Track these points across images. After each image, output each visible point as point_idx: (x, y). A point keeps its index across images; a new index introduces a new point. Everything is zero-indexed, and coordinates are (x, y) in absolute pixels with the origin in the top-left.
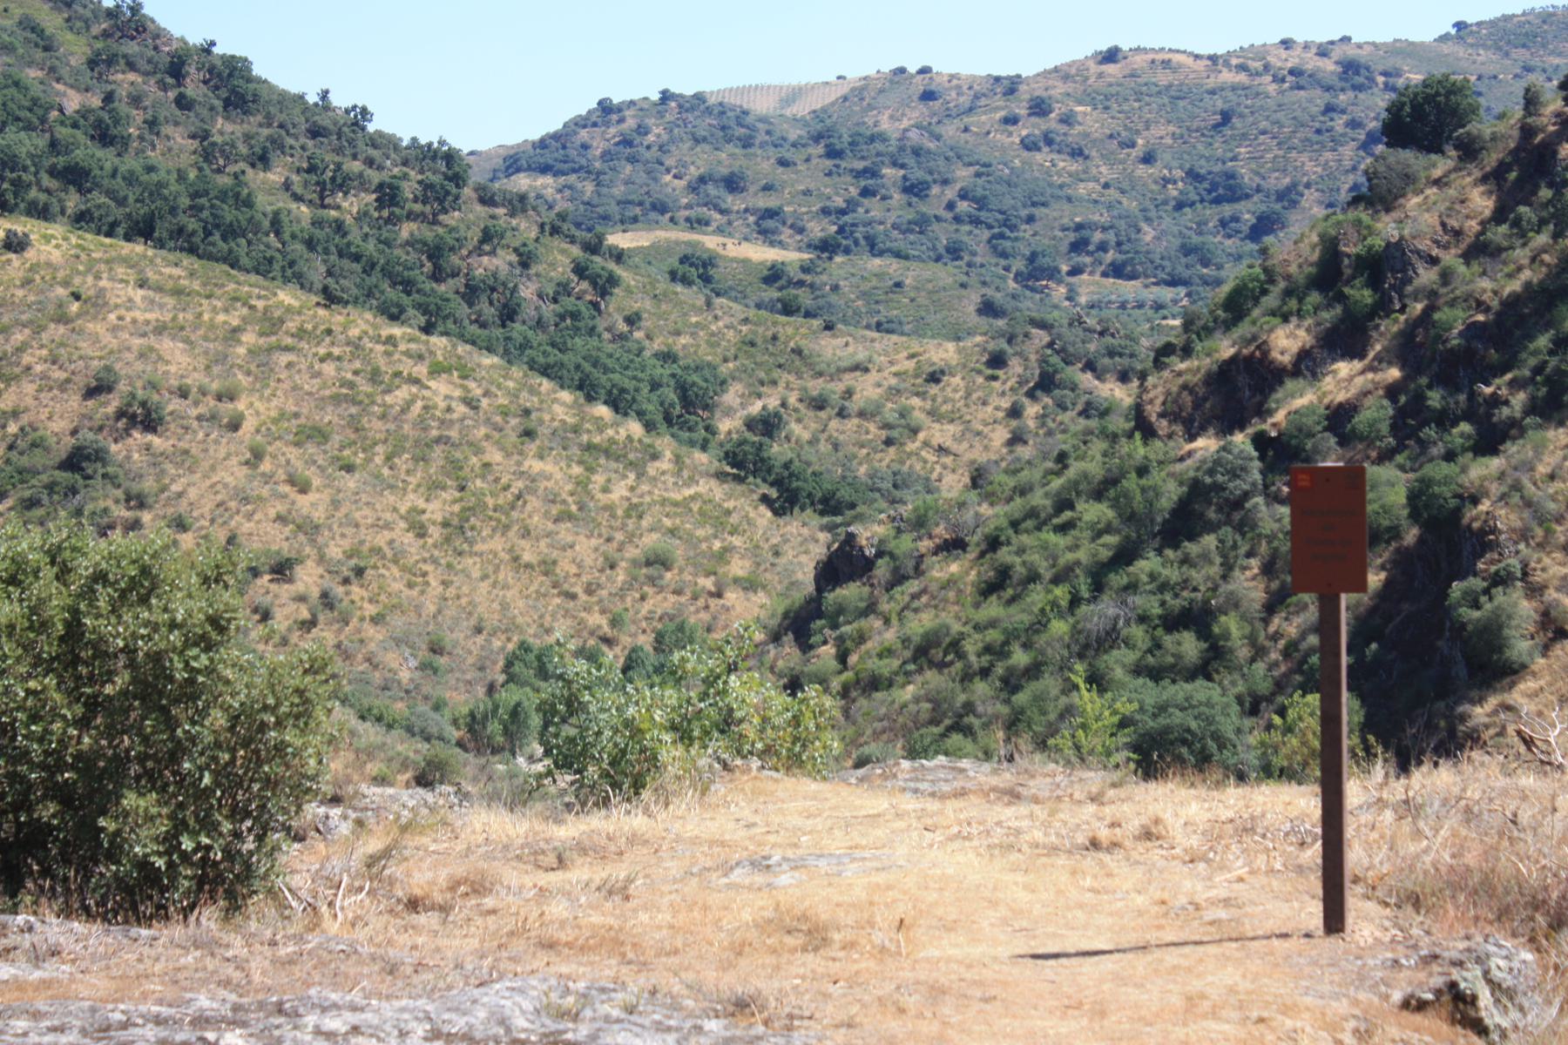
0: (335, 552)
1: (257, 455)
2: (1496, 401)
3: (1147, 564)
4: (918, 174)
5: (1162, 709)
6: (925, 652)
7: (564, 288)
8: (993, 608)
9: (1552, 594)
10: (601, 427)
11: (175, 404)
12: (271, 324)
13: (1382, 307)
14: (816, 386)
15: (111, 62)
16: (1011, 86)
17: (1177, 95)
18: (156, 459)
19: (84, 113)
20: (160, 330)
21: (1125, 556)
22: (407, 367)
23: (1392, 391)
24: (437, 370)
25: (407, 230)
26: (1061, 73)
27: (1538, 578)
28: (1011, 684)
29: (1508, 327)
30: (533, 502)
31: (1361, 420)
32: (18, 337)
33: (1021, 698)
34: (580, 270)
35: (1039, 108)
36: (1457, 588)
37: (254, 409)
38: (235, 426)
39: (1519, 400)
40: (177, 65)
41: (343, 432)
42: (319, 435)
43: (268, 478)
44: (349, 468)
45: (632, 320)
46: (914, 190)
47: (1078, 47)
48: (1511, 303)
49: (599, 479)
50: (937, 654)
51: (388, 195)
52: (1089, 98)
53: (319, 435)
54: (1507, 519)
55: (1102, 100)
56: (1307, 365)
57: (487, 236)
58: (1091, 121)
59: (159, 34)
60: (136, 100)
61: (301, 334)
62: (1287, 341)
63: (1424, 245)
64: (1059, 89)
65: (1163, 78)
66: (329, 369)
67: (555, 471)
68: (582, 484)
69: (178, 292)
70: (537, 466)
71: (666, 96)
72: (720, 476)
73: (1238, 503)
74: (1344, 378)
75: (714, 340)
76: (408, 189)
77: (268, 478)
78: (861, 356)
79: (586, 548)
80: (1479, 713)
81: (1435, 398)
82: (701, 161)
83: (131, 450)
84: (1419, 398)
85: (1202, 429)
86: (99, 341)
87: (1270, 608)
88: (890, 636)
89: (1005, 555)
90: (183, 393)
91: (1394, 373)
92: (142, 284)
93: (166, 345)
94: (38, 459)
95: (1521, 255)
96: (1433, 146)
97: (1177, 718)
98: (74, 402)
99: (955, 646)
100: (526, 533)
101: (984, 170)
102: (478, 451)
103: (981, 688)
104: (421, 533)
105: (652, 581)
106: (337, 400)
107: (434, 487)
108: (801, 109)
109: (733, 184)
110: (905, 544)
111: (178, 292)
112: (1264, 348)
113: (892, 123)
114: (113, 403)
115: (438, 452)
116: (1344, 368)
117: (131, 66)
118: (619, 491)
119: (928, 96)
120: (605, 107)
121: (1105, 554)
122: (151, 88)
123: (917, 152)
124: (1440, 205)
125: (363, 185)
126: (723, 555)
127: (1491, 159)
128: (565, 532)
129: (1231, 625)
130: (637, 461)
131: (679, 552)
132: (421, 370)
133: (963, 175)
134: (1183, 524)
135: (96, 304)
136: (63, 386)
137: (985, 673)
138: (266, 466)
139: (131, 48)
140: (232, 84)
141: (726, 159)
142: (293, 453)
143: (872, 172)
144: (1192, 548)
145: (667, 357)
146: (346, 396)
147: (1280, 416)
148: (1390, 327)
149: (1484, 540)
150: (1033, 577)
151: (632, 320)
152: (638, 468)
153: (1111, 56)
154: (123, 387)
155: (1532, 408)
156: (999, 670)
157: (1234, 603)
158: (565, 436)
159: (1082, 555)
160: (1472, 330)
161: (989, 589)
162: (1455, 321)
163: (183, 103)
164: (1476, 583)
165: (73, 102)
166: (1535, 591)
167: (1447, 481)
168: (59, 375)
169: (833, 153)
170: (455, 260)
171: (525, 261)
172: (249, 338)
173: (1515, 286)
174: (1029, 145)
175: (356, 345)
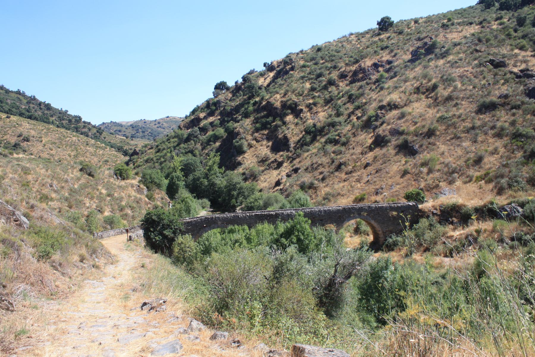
0: (56, 158)
1: (45, 145)
2: (236, 117)
3: (182, 145)
4: (144, 130)
5: (187, 160)
6: (147, 161)
7: (95, 133)
8: (158, 154)
9: (249, 141)
10: (98, 144)
11: (32, 138)
12: (48, 129)
13: (217, 109)
14: (130, 147)
15: (30, 103)
16: (155, 121)
17: (176, 122)
18: (28, 146)
19: (25, 108)
20: (31, 129)
21: (178, 145)
22: (69, 136)
23: (219, 119)
24: (74, 136)
25: (73, 126)
26: (162, 119)
27: (247, 139)
28: (161, 163)
29: (237, 109)
30: (88, 153)
31: (215, 123)
32: (7, 129)
33: (163, 165)
34: (97, 132)
35: (159, 123)
36: (234, 141)
37: (44, 140)
38: (41, 141)
39: (240, 117)
40: (40, 104)
41: (59, 143)
42: (55, 143)
43: (46, 149)
44: (59, 148)
45: (105, 138)
46: (143, 132)
47: (164, 116)
48: (237, 105)
49: (98, 151)
50: (149, 161)
51: (70, 121)
52: (165, 122)
53: (55, 143)
54: (241, 131)
55: (167, 122)
56: (205, 118)
57: (84, 127)
58: (165, 125)
59: (37, 100)
60: (34, 108)
61: (53, 131)
62: (202, 115)
63: (222, 101)
64: (161, 121)
65: (174, 120)
66: (57, 135)
67: (91, 149)
68: (95, 151)
69: (34, 125)
70: (88, 148)
71: (111, 122)
72: (116, 151)
73: (196, 137)
74: (211, 119)
75: (116, 141)
76: (73, 120)
77: (46, 149)
78: (137, 143)
79: (96, 159)
80: (240, 159)
81: (226, 119)
82: (116, 128)
83: (25, 144)
84: (224, 119)
85: (189, 128)
86: (20, 130)
87: (202, 150)
88: (141, 160)
89: (159, 147)
90: (33, 137)
91: (219, 117)
92: (28, 123)
93: (31, 131)
94: (9, 145)
95: (238, 100)
96: (222, 89)
97: (190, 161)
98: (16, 138)
99: (152, 159)
100: (87, 157)
101: (152, 130)
102: (80, 146)
103: (156, 164)
104: (70, 156)
105: (106, 164)
106: (58, 139)
107: (73, 151)
108: (129, 124)
109: (120, 131)
110: (144, 149)
111: (34, 125)
112: (199, 116)
113: (140, 125)
114: (22, 138)
115: (73, 146)
116: (211, 118)
117: (33, 104)
118: (101, 152)
119: (145, 122)
120: (103, 123)
121: (175, 145)
122: (36, 107)
123: (144, 127)
124: (224, 96)
125: (67, 120)
126: (117, 161)
127: (231, 90)
128: (93, 157)
129: (197, 152)
130: (104, 149)
131: (110, 160)
132: (71, 136)
133: (150, 130)
134: (188, 140)
135: (21, 125)
136: (14, 136)
137: (157, 162)
138: (46, 147)
139: (33, 102)
140: (48, 107)
141: (119, 128)
142: (50, 146)
143: (138, 130)
144: (189, 143)
145: (110, 142)
146: (60, 138)
147: (202, 125)
148: (218, 112)
149: (238, 134)
150: (164, 149)
151: (105, 138)
152: (104, 150)
153: (168, 117)
154: (24, 136)
155: (242, 117)
156: (159, 161)
157: (196, 149)
158: (93, 145)
159: (172, 145)
160: (231, 109)
161: (158, 152)
162: (228, 108)
163: (41, 109)
164: (238, 139)
165: (23, 107)
166: (247, 141)
167: (231, 126)
168: (13, 134)
169: (133, 128)
170: (79, 129)
171: (90, 129)
172: (45, 131)
173: (238, 103)
174: (158, 127)
175: (62, 132)
